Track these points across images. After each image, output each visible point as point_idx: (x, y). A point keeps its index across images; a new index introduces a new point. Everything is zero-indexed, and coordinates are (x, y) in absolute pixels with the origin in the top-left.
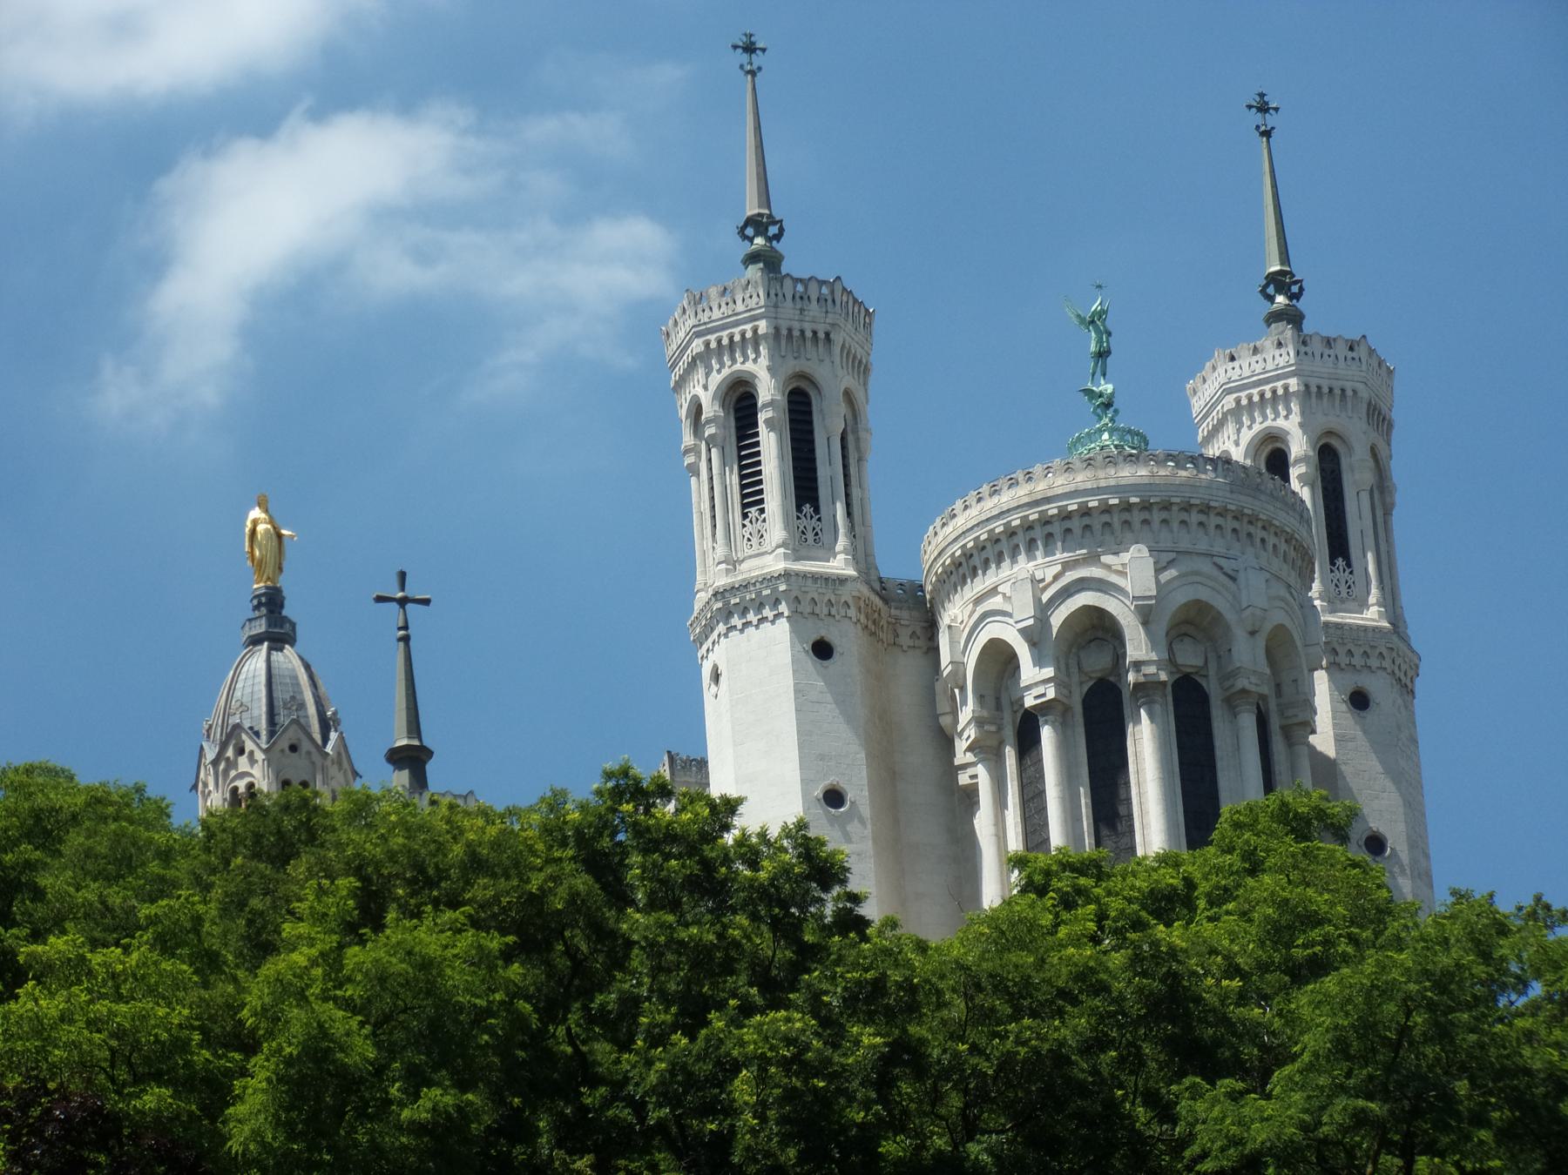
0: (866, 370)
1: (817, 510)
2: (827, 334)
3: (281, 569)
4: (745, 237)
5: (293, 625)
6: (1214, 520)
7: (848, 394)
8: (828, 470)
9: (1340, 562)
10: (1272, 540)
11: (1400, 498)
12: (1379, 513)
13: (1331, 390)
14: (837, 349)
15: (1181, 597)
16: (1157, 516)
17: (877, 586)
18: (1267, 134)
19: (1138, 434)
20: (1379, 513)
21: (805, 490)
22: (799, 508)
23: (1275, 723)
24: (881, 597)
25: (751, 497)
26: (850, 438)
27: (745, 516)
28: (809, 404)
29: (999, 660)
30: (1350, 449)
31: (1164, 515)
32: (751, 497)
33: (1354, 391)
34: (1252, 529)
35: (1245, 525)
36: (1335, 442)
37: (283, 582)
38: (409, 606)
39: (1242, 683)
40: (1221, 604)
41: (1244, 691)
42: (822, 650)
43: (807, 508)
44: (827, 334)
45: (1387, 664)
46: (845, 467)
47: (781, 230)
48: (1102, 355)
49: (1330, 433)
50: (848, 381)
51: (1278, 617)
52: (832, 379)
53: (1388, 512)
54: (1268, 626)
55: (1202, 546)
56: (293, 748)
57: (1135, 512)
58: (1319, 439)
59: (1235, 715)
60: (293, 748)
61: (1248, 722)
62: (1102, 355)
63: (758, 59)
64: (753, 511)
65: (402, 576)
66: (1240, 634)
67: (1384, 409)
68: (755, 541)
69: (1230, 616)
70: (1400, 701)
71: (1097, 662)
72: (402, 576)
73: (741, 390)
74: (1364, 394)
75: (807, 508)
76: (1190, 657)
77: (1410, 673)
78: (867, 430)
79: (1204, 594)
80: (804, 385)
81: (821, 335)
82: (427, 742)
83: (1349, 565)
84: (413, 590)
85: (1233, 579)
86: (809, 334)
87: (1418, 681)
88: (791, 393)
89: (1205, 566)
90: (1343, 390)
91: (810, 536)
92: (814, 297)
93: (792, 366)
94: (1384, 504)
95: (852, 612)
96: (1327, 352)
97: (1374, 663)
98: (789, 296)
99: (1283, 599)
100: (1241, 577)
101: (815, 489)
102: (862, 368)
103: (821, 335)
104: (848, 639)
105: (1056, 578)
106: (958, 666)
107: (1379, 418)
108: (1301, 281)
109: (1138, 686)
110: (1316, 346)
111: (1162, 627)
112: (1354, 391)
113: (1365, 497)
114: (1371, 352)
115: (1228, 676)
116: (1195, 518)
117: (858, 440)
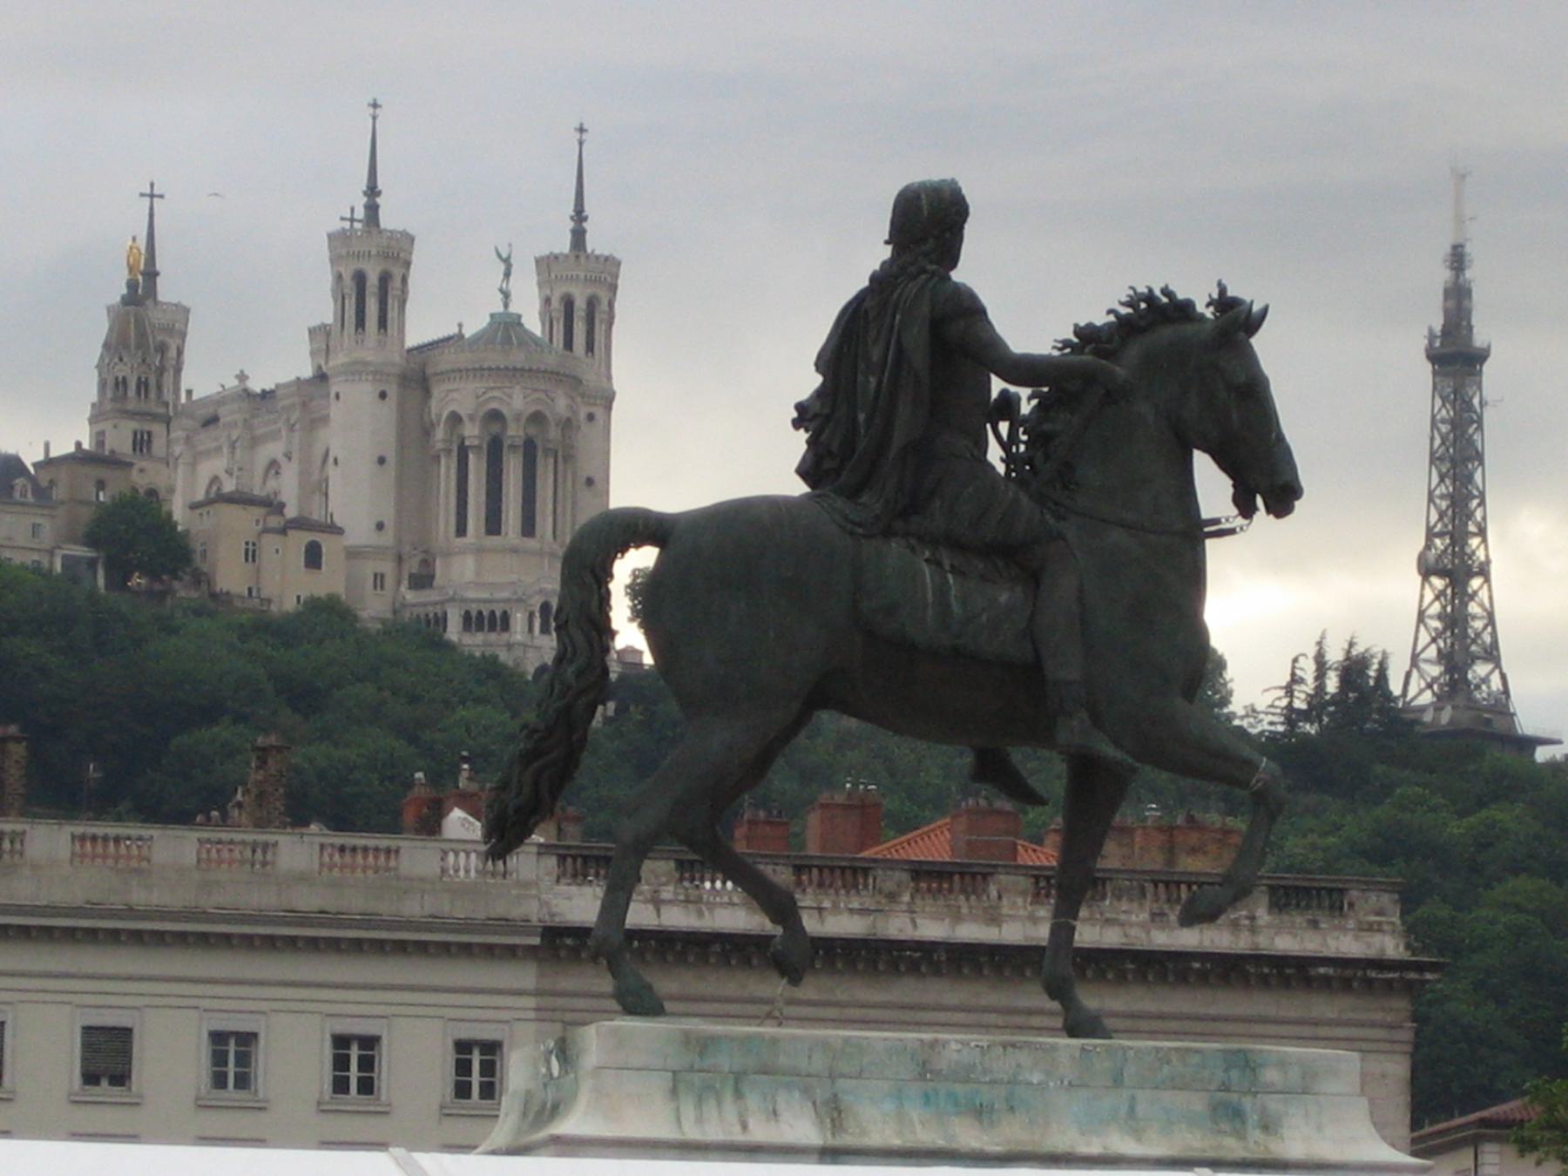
8: (392, 314)
11: (617, 320)
15: (532, 409)
23: (560, 454)
25: (360, 322)
27: (356, 330)
29: (455, 419)
32: (360, 322)
33: (605, 279)
39: (550, 446)
41: (550, 449)
42: (383, 395)
43: (382, 331)
48: (507, 275)
50: (404, 270)
52: (397, 272)
61: (551, 461)
62: (507, 275)
63: (378, 111)
64: (360, 330)
65: (152, 185)
71: (495, 428)
72: (152, 185)
76: (532, 431)
79: (539, 408)
82: (158, 267)
89: (543, 396)
104: (393, 391)
105: (484, 393)
106: (439, 416)
107: (613, 288)
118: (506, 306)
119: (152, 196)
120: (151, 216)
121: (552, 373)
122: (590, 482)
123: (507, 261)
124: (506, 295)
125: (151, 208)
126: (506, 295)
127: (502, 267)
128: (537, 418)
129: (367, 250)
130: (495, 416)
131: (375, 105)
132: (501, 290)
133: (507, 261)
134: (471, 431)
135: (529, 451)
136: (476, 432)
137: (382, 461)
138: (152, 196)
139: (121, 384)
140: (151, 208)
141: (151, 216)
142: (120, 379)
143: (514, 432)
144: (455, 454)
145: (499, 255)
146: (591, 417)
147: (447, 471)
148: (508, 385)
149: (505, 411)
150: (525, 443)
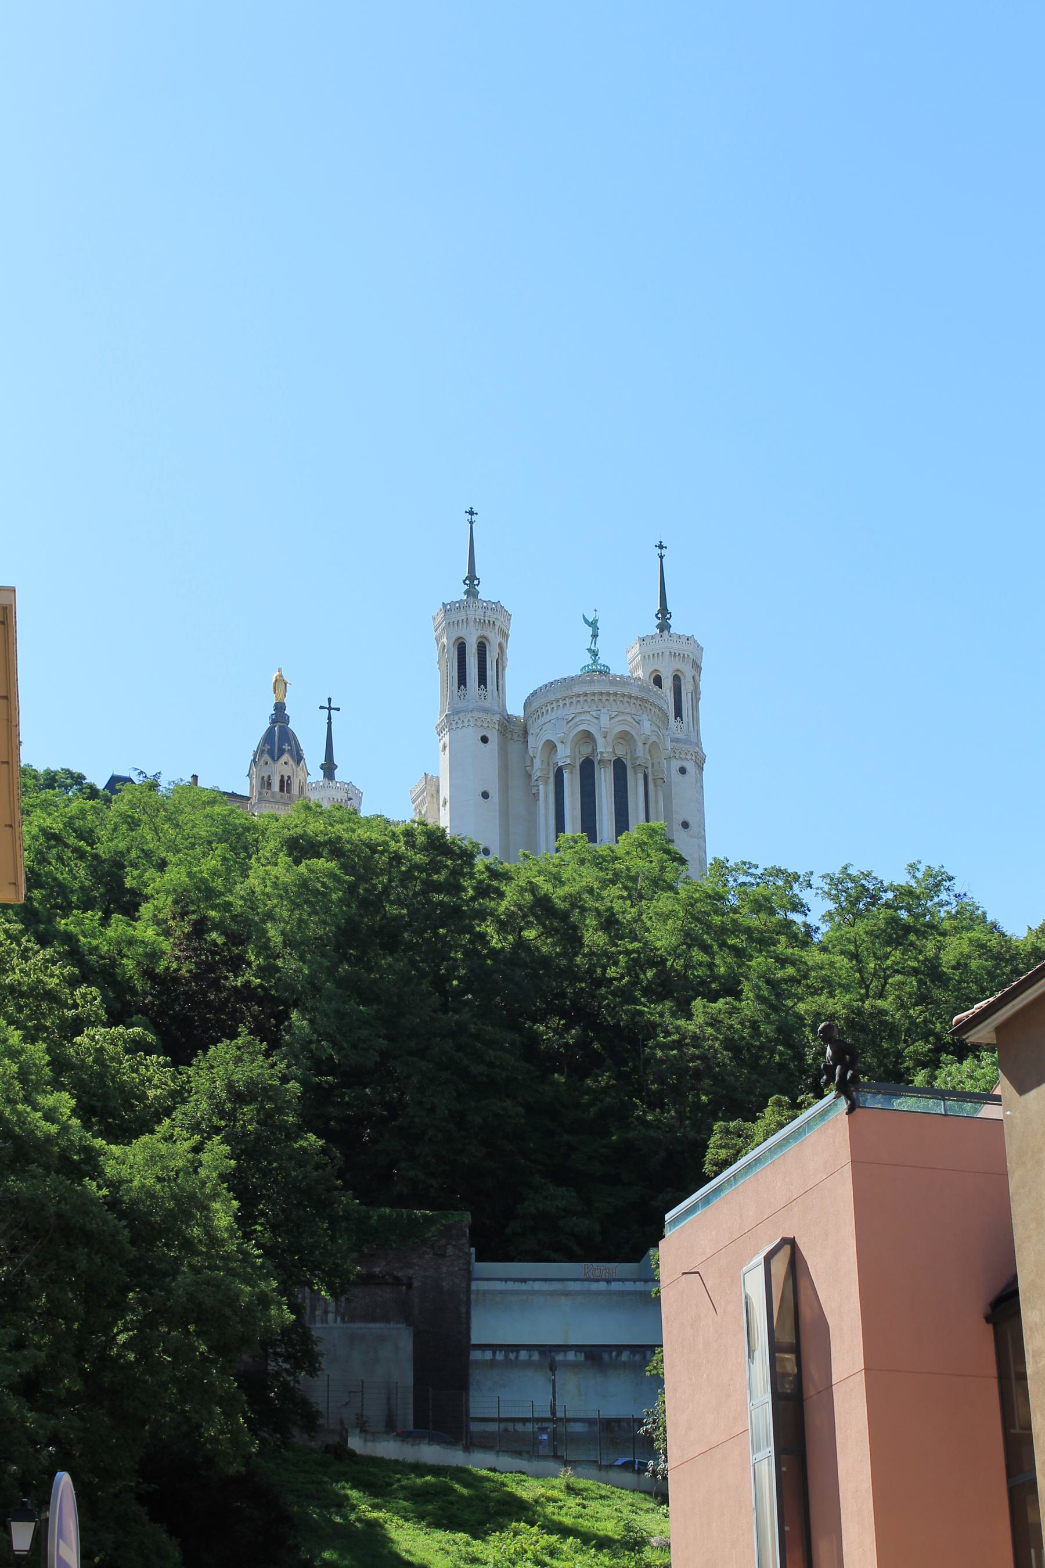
0: (508, 636)
1: (486, 688)
2: (494, 622)
3: (285, 696)
4: (465, 584)
5: (289, 717)
6: (633, 701)
7: (500, 645)
8: (491, 673)
9: (678, 719)
10: (653, 709)
12: (694, 702)
13: (679, 654)
14: (497, 628)
16: (612, 698)
17: (506, 718)
18: (661, 557)
19: (607, 667)
20: (694, 702)
21: (482, 680)
22: (479, 687)
23: (650, 778)
24: (508, 722)
25: (462, 680)
26: (500, 661)
27: (459, 688)
28: (485, 648)
29: (551, 747)
30: (685, 677)
31: (614, 698)
32: (462, 680)
34: (646, 705)
35: (643, 702)
36: (679, 674)
37: (285, 701)
38: (332, 711)
40: (633, 732)
42: (485, 740)
43: (482, 686)
44: (494, 622)
45: (694, 758)
46: (497, 672)
47: (479, 582)
48: (595, 636)
49: (678, 670)
50: (500, 639)
51: (654, 738)
52: (494, 639)
53: (698, 701)
54: (650, 742)
55: (628, 711)
56: (286, 763)
57: (604, 696)
58: (674, 672)
59: (636, 774)
60: (286, 763)
61: (641, 776)
62: (595, 636)
63: (474, 517)
65: (330, 700)
66: (640, 744)
67: (699, 663)
68: (462, 697)
69: (636, 737)
70: (697, 772)
71: (586, 751)
72: (330, 700)
73: (460, 641)
74: (691, 657)
75: (482, 686)
76: (621, 752)
77: (702, 762)
78: (507, 659)
79: (627, 728)
80: (484, 640)
81: (491, 622)
83: (682, 720)
84: (332, 706)
85: (639, 723)
86: (487, 622)
87: (705, 764)
88: (479, 643)
89: (629, 718)
90: (684, 655)
91: (483, 697)
92: (489, 609)
93: (480, 633)
94: (696, 697)
95: (497, 726)
96: (678, 640)
97: (689, 757)
98: (480, 608)
99: (657, 732)
100: (641, 723)
101: (486, 679)
102: (505, 635)
103: (491, 622)
104: (493, 737)
107: (697, 667)
108: (670, 613)
109: (600, 761)
110: (675, 638)
111: (610, 738)
112: (688, 656)
113: (690, 695)
114: (695, 641)
115: (634, 759)
116: (626, 699)
117: (502, 662)
118: (595, 661)
119: (330, 709)
120: (329, 724)
121: (637, 698)
122: (685, 825)
123: (593, 624)
124: (595, 654)
125: (329, 718)
126: (595, 654)
127: (590, 630)
128: (625, 737)
129: (464, 618)
130: (587, 737)
131: (471, 513)
132: (589, 650)
133: (593, 624)
134: (564, 755)
135: (620, 769)
136: (568, 752)
137: (485, 795)
138: (330, 709)
139: (267, 783)
140: (329, 718)
141: (329, 724)
142: (266, 779)
143: (604, 749)
144: (552, 780)
145: (586, 621)
146: (683, 771)
147: (546, 793)
148: (596, 709)
149: (593, 731)
150: (615, 762)
